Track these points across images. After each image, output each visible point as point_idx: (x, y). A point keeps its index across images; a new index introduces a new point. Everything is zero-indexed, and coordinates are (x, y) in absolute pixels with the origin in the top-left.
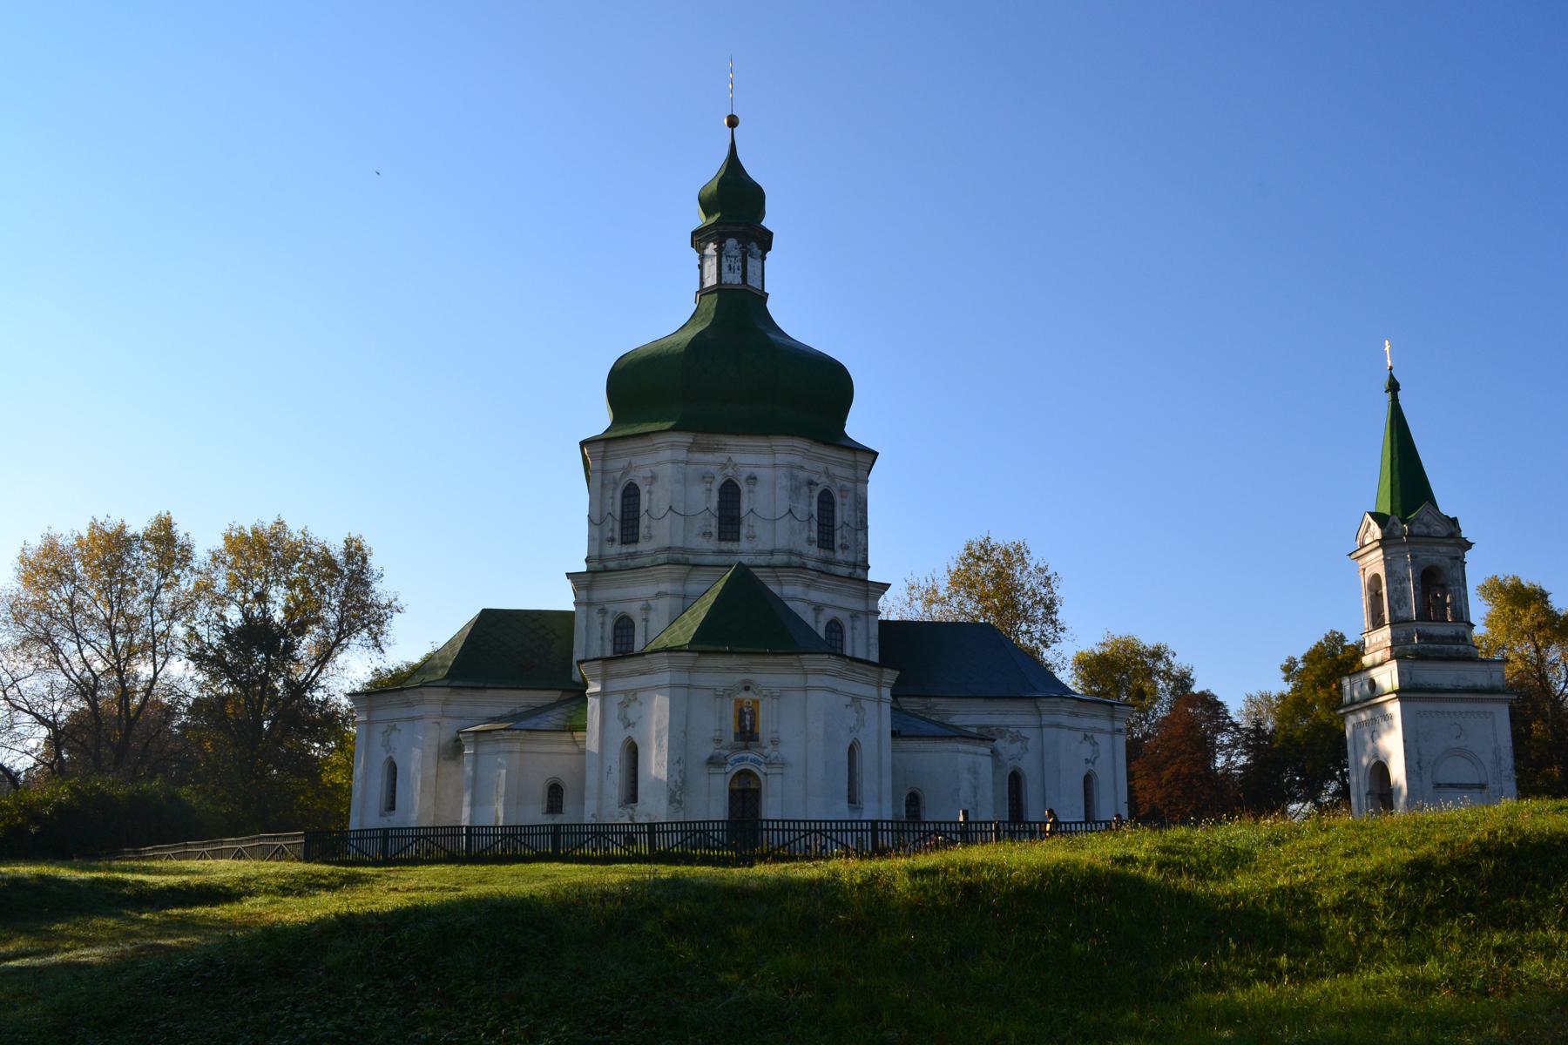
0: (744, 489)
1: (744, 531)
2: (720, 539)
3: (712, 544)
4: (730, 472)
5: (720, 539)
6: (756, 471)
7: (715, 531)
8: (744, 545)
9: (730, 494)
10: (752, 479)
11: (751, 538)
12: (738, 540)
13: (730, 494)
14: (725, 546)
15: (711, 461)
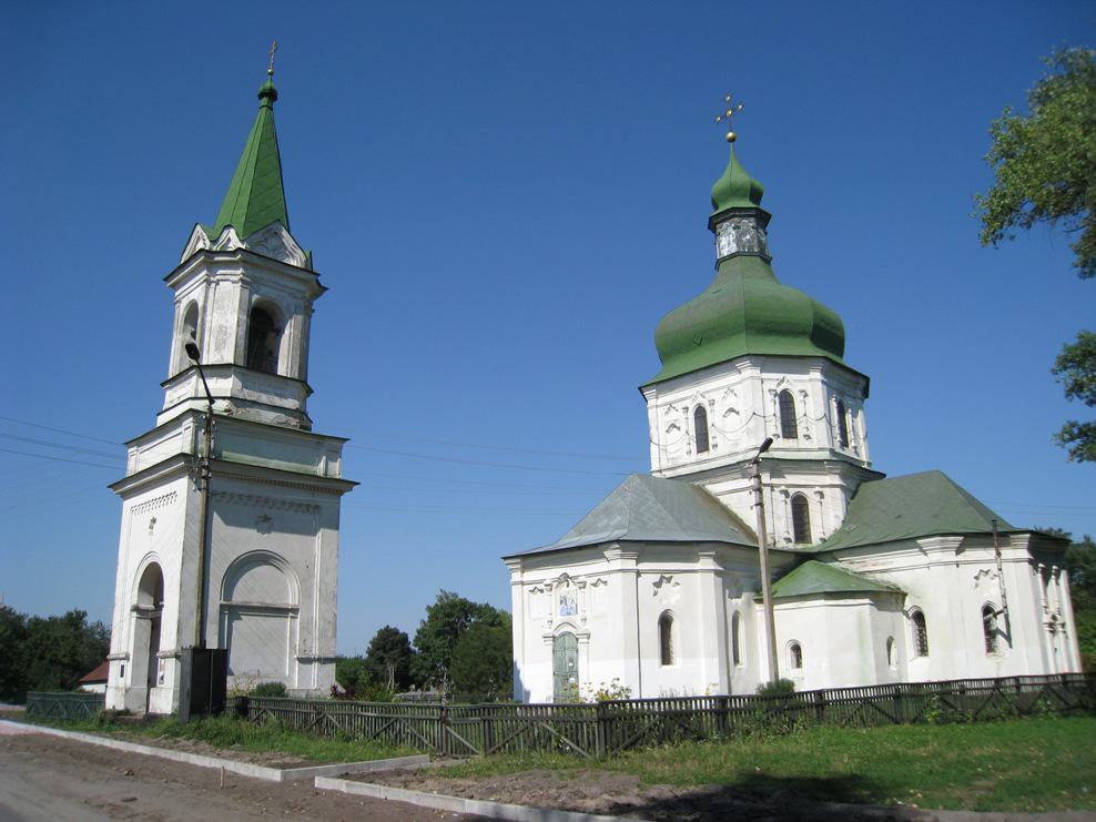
0: (708, 409)
1: (711, 442)
2: (698, 452)
3: (695, 457)
4: (700, 400)
5: (698, 452)
6: (711, 396)
7: (694, 447)
8: (712, 453)
9: (700, 414)
10: (712, 403)
11: (715, 446)
12: (707, 449)
13: (700, 414)
14: (704, 456)
15: (688, 395)
